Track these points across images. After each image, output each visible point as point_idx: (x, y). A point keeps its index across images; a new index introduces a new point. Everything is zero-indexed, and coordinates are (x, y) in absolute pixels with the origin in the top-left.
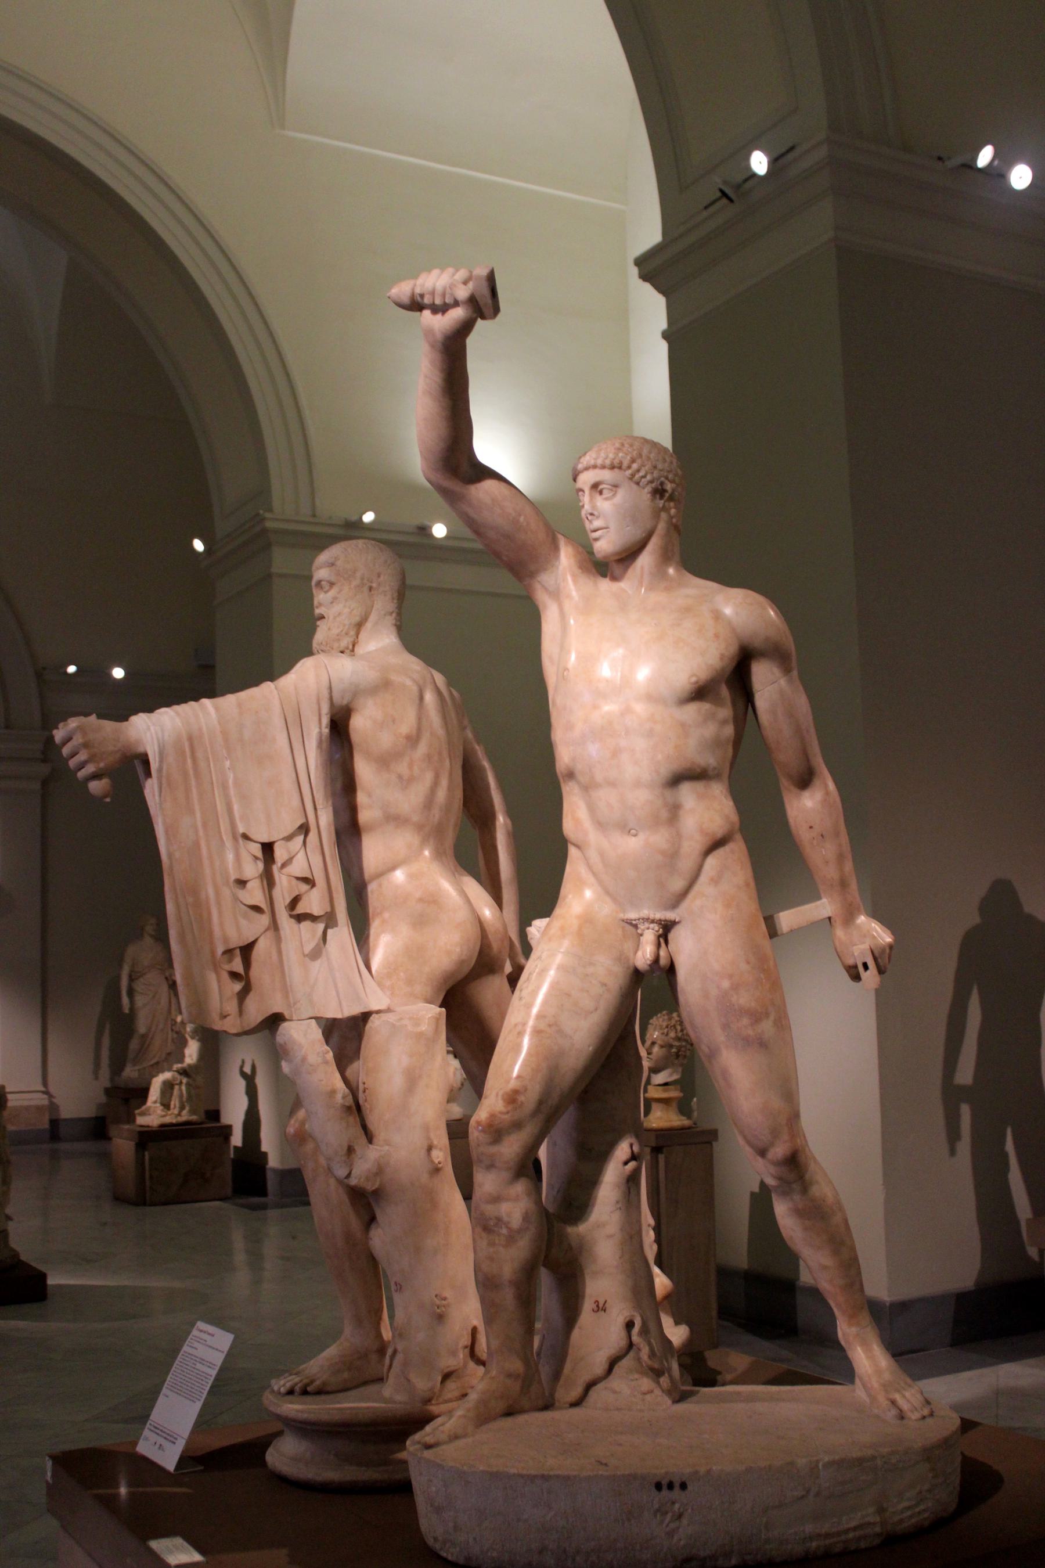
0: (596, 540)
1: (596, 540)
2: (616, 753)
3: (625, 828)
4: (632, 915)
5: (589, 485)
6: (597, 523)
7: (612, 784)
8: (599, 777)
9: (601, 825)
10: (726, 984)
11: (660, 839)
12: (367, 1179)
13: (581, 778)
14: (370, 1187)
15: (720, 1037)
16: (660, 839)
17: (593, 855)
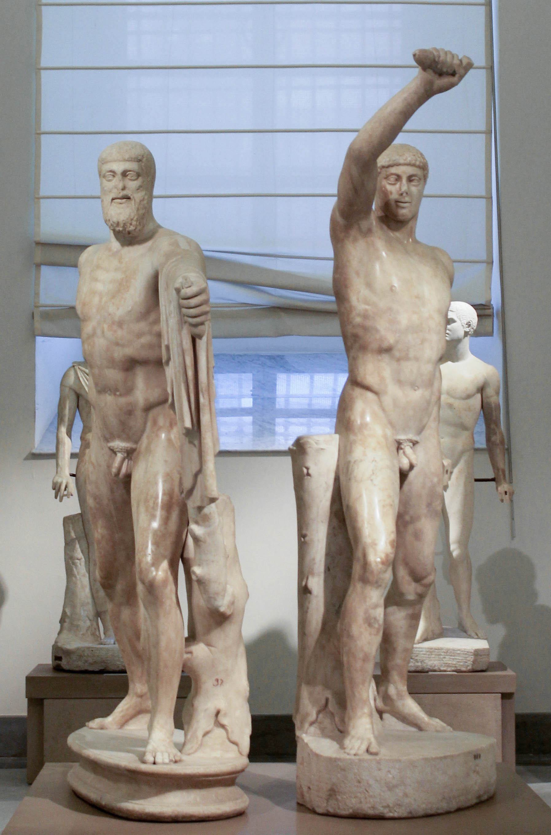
0: (403, 208)
1: (403, 208)
2: (423, 341)
3: (414, 386)
4: (402, 437)
5: (408, 175)
6: (407, 199)
7: (417, 359)
8: (412, 354)
9: (400, 382)
10: (435, 480)
11: (427, 393)
12: (229, 607)
13: (397, 354)
14: (229, 612)
15: (423, 510)
16: (427, 393)
17: (387, 400)
